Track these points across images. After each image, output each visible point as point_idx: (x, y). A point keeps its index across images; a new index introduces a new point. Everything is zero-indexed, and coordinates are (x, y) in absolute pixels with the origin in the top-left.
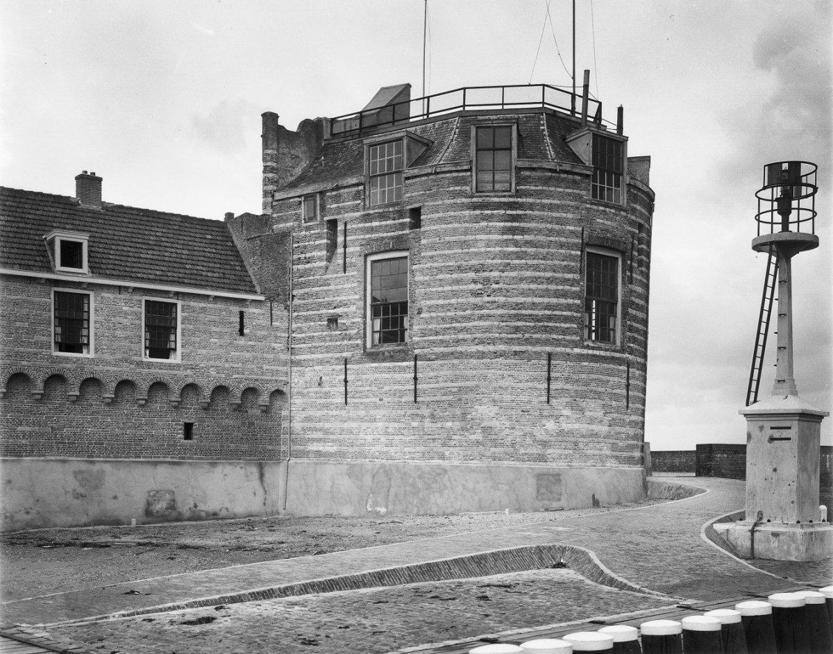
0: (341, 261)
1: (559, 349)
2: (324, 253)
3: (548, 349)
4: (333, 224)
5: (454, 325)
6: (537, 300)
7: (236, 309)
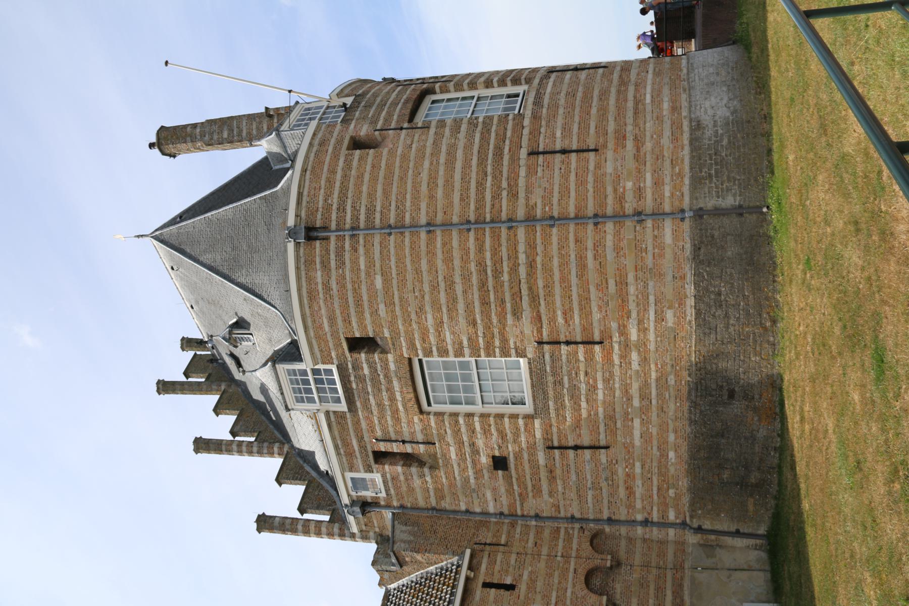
0: (422, 448)
1: (525, 142)
2: (414, 470)
3: (523, 153)
4: (380, 457)
5: (491, 288)
6: (457, 176)
7: (478, 592)
